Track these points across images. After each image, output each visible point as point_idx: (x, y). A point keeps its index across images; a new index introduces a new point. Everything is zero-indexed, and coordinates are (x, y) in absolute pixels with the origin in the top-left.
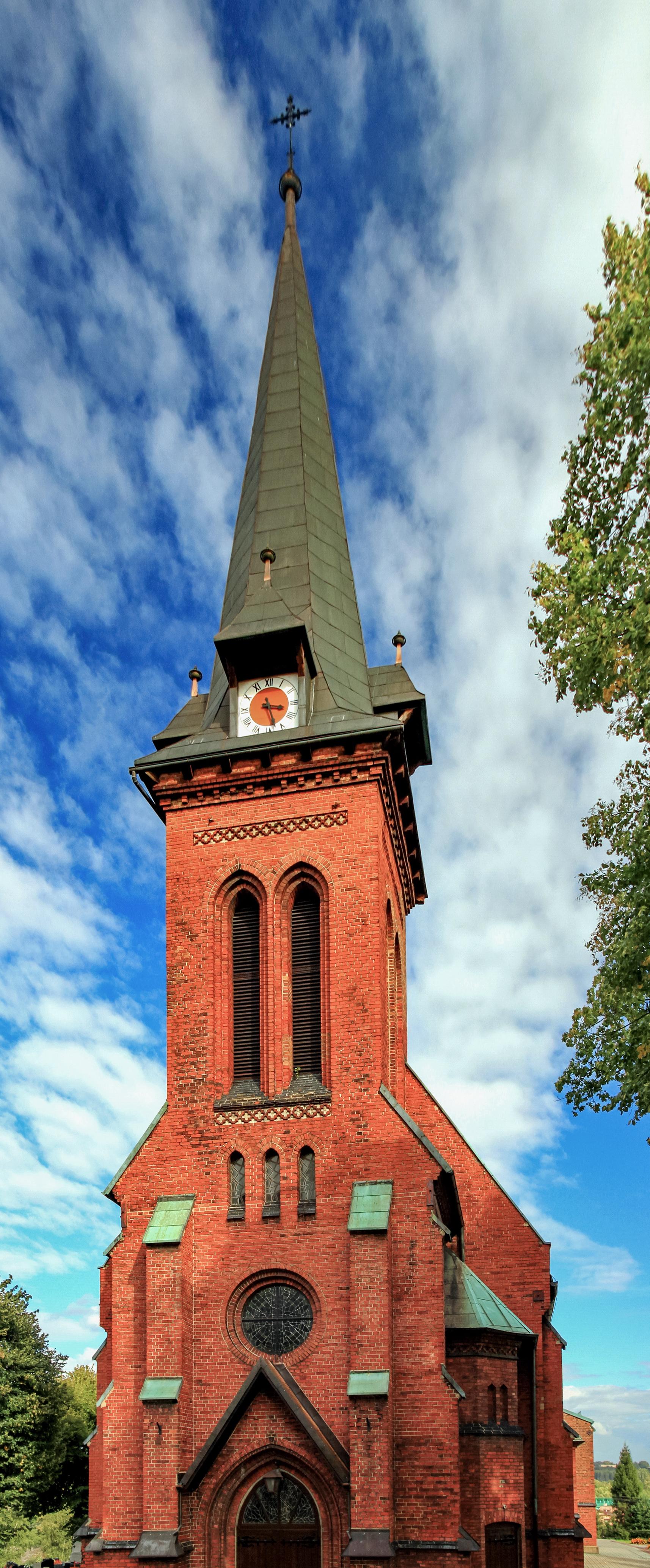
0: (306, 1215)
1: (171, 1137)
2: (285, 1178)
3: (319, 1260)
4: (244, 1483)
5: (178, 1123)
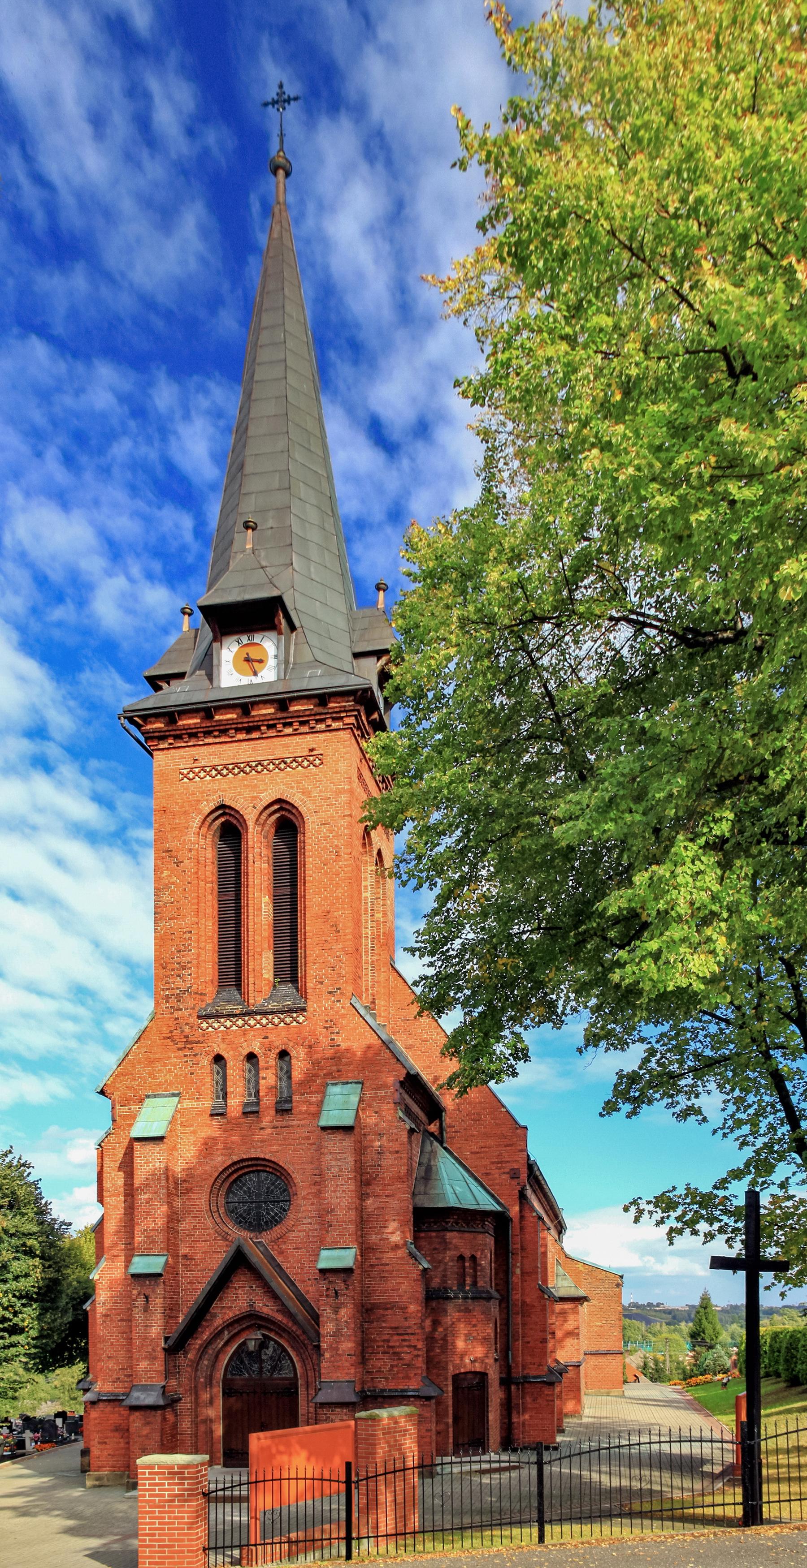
0: (283, 1111)
2: (264, 1078)
3: (295, 1150)
4: (227, 1343)
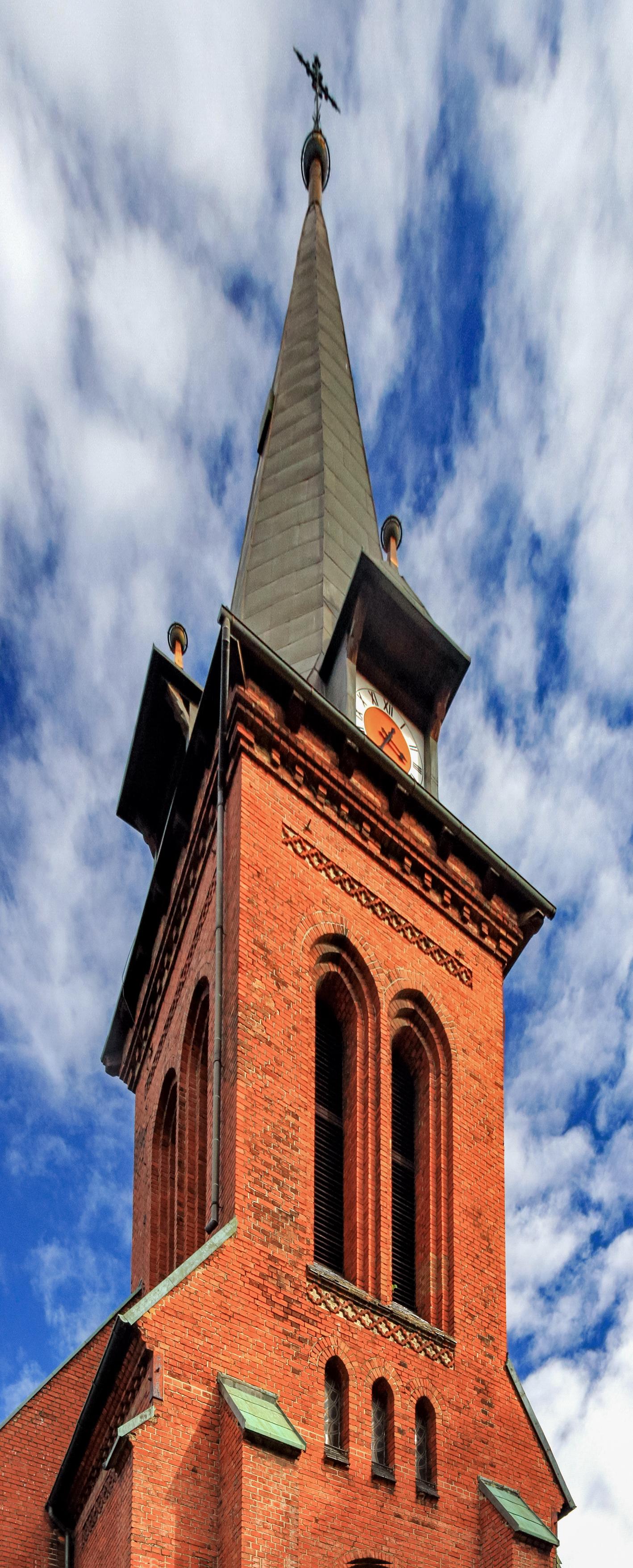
1: (241, 1283)
5: (252, 1265)
